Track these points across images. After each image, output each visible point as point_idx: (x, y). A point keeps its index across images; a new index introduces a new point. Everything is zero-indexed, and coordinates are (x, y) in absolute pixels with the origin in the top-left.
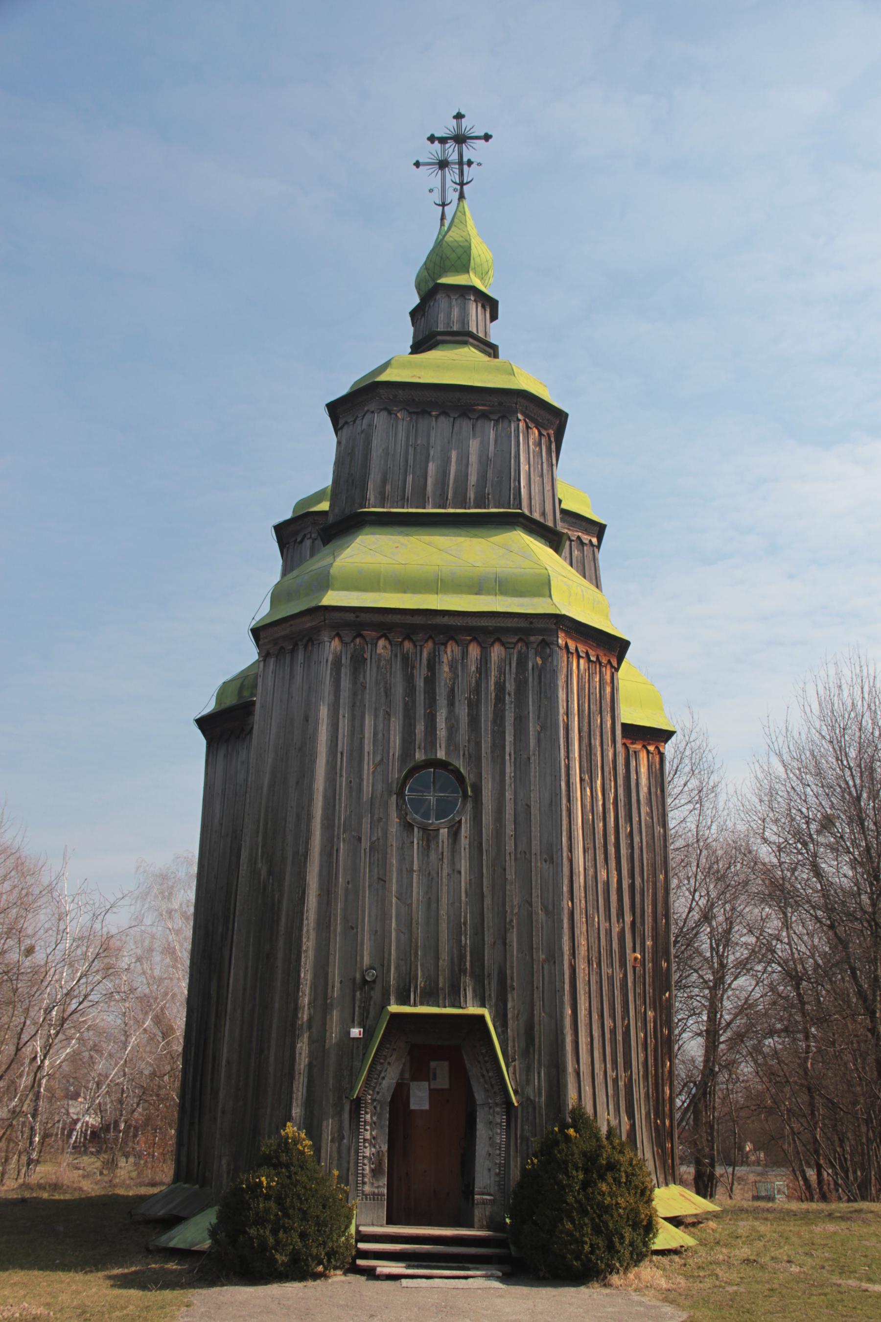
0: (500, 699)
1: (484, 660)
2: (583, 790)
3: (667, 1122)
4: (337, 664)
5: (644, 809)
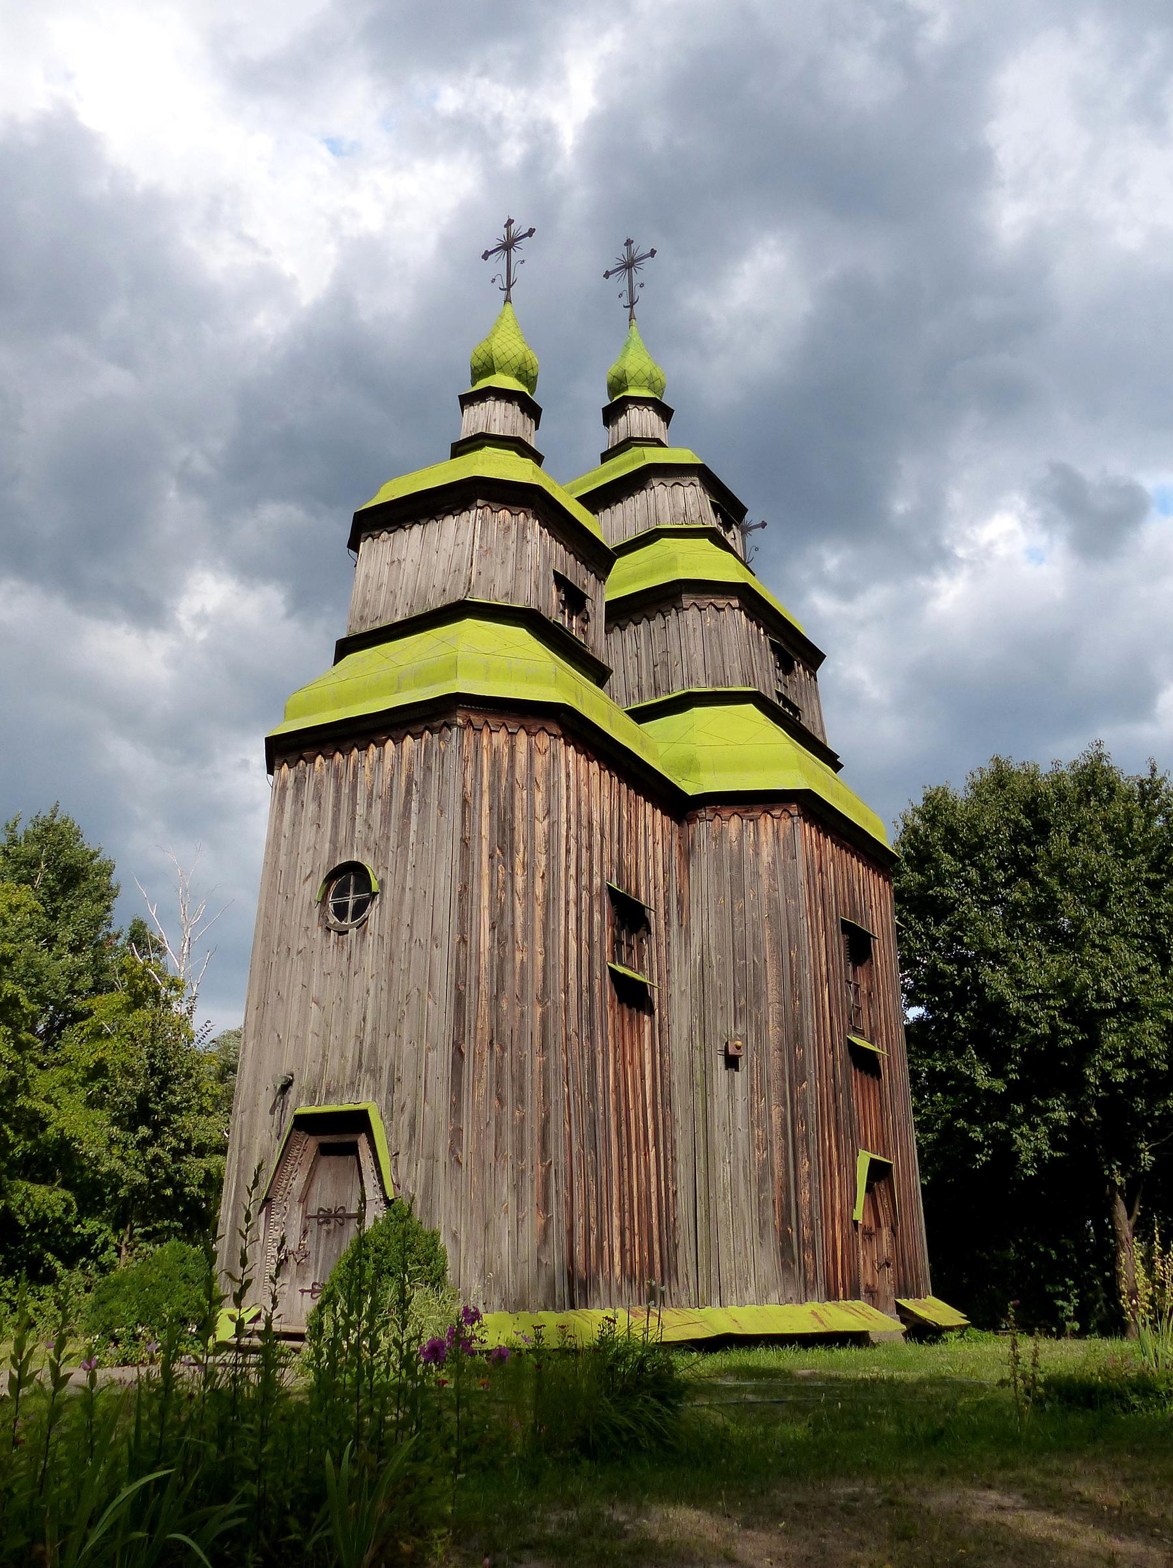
0: (408, 792)
1: (399, 757)
3: (806, 1232)
5: (765, 881)
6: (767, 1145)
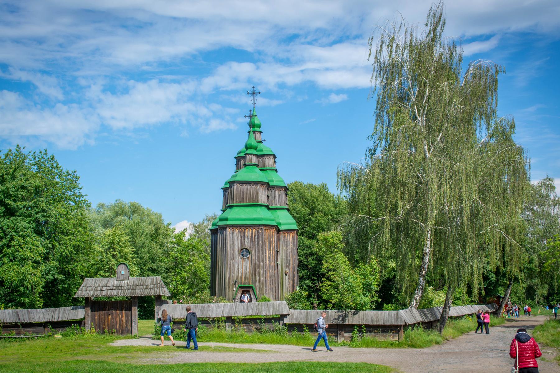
0: (255, 238)
2: (268, 251)
4: (230, 233)
5: (291, 244)
6: (289, 287)
